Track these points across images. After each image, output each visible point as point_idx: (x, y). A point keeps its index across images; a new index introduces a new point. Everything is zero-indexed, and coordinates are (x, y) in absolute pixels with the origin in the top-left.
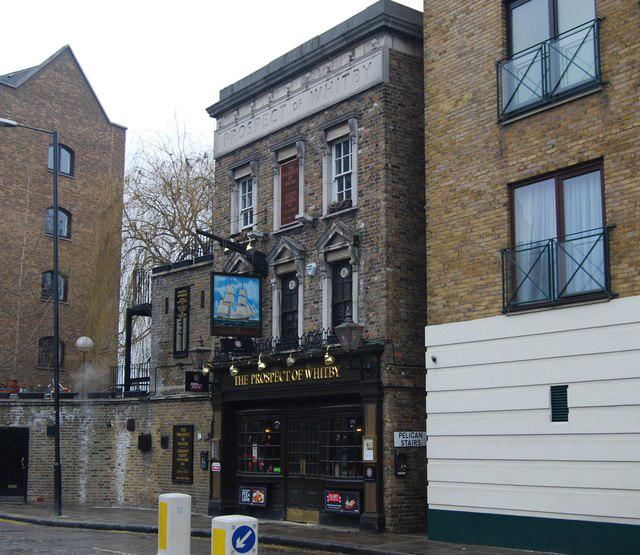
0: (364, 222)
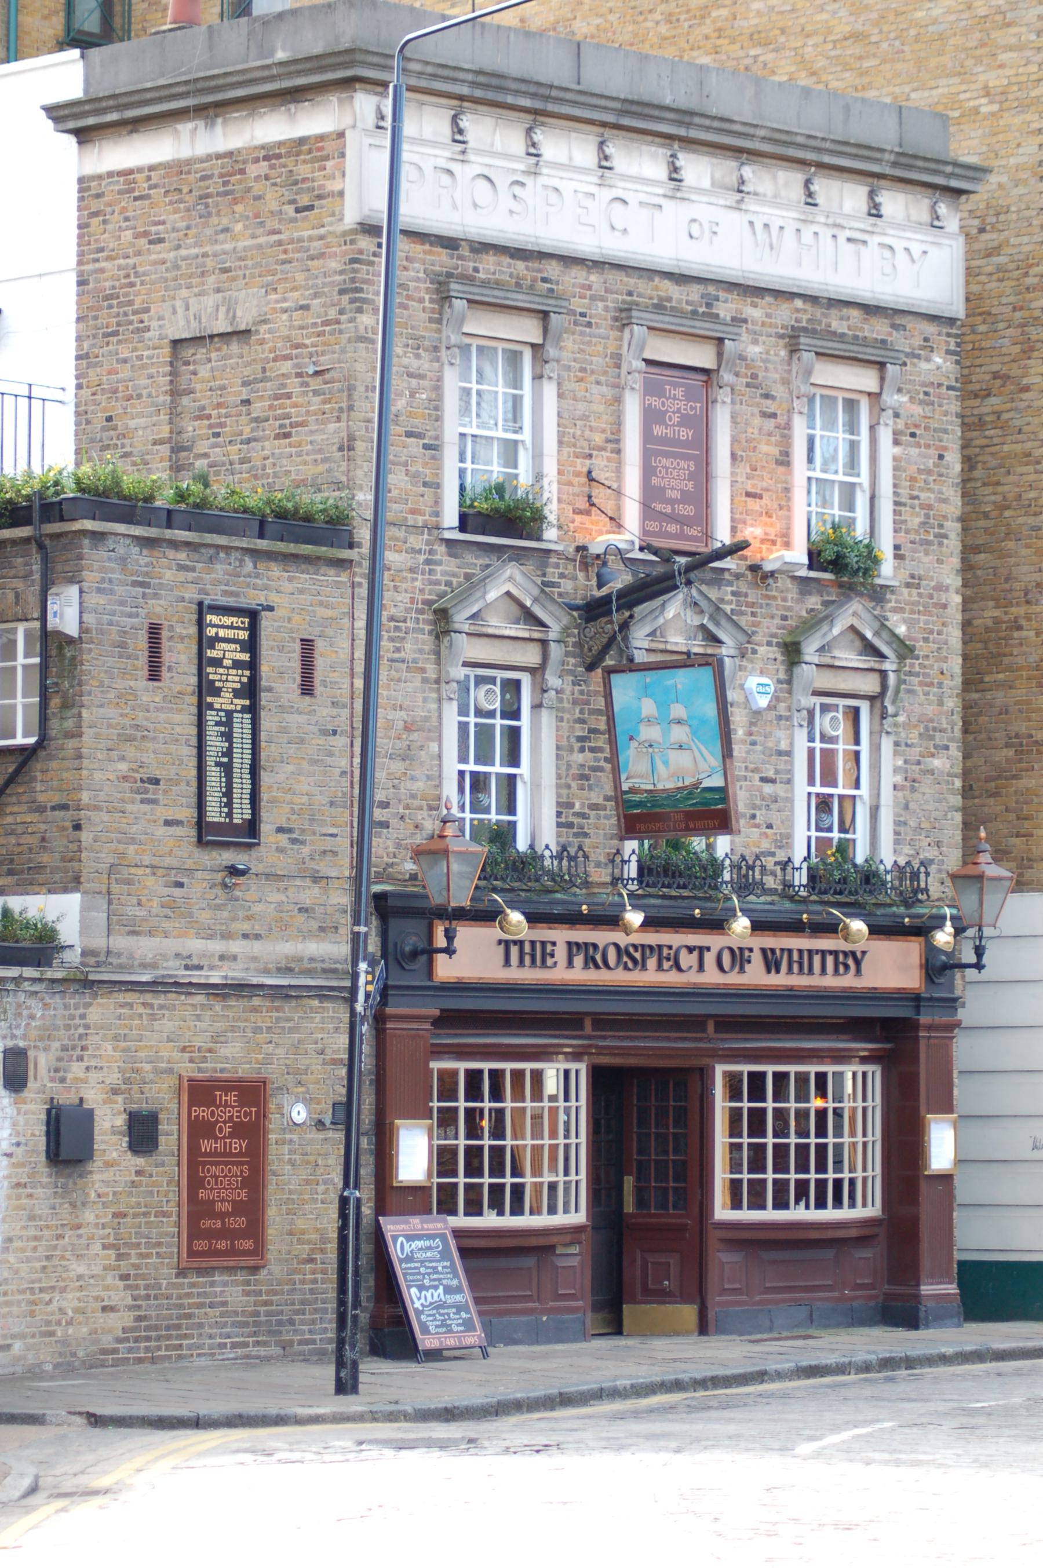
0: (910, 624)
